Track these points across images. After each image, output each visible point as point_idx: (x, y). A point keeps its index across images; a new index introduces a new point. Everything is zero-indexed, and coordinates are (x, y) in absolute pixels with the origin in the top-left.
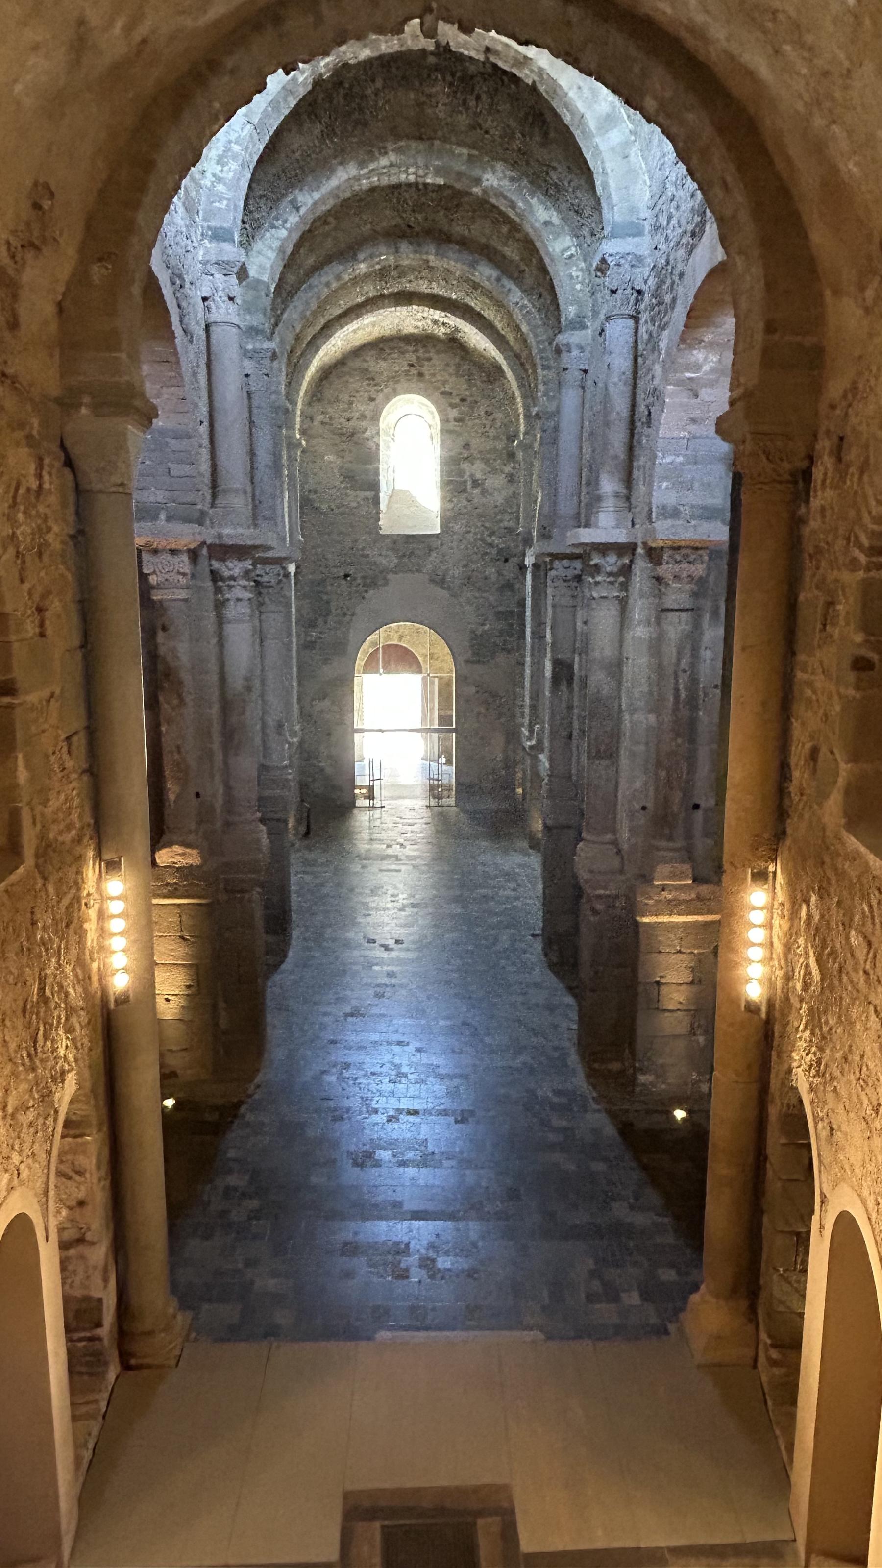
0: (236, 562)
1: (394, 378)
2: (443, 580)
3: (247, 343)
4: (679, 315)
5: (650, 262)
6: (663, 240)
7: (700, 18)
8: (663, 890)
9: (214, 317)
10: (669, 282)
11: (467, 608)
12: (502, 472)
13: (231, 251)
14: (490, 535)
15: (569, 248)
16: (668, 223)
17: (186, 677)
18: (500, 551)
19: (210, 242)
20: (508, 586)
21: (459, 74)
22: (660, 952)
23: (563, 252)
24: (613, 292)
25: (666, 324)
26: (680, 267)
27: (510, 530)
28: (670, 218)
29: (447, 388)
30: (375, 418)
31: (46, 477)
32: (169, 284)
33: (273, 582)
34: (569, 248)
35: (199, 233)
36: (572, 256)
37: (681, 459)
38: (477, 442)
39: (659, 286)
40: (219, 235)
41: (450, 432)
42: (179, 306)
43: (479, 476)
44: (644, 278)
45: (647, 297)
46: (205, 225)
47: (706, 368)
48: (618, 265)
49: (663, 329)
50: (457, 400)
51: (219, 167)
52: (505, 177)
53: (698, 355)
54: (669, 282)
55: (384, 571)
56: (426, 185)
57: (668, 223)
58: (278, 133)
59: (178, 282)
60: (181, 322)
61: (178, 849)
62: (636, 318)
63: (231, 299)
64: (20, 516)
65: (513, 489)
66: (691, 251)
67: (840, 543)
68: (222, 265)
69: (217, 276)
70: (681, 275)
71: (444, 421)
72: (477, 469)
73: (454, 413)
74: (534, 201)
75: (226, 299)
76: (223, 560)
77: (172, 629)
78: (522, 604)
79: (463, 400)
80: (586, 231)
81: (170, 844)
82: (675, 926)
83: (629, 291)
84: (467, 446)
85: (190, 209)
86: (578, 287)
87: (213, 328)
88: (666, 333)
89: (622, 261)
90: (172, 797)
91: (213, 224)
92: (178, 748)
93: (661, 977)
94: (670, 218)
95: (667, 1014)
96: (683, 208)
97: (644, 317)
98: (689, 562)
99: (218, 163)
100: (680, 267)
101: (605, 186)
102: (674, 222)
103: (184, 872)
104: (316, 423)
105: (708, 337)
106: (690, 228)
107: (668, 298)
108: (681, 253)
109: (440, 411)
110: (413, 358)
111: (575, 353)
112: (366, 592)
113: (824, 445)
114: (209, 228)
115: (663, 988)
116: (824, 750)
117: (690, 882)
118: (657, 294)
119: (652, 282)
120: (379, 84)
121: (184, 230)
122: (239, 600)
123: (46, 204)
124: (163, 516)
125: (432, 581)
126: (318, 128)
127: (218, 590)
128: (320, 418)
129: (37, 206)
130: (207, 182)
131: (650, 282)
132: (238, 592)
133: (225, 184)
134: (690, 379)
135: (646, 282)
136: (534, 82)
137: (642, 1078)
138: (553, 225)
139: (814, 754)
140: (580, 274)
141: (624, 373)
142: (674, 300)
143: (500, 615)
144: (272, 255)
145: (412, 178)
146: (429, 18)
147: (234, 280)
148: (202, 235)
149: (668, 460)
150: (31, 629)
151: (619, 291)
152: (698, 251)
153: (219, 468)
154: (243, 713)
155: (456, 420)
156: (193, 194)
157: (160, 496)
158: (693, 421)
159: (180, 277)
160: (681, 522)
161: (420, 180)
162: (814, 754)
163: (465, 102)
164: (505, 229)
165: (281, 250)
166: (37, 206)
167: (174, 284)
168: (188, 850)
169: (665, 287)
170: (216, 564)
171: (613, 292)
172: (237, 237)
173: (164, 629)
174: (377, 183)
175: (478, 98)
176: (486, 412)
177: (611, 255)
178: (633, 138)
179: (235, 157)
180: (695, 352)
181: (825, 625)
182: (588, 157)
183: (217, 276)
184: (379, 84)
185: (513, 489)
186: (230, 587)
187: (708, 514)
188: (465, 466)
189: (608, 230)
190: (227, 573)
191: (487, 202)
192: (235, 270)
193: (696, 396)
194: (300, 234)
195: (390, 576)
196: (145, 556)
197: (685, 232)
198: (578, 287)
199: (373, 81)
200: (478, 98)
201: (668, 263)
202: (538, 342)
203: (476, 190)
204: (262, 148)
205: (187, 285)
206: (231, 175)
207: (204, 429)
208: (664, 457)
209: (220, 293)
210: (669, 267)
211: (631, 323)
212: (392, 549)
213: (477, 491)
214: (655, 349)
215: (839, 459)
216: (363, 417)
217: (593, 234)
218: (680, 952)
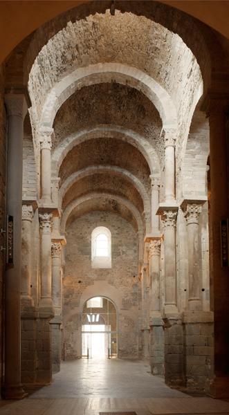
18: (132, 274)
20: (136, 285)
27: (135, 267)
30: (90, 233)
47: (197, 148)
55: (93, 280)
71: (112, 234)
72: (124, 248)
73: (116, 232)
76: (43, 214)
77: (26, 229)
78: (140, 290)
87: (43, 151)
110: (102, 215)
111: (156, 180)
125: (109, 283)
127: (41, 224)
143: (133, 294)
144: (60, 154)
153: (43, 189)
163: (120, 108)
165: (63, 154)
170: (41, 216)
173: (23, 229)
195: (95, 282)
200: (124, 106)
203: (123, 139)
207: (39, 176)
212: (96, 273)
213: (124, 255)
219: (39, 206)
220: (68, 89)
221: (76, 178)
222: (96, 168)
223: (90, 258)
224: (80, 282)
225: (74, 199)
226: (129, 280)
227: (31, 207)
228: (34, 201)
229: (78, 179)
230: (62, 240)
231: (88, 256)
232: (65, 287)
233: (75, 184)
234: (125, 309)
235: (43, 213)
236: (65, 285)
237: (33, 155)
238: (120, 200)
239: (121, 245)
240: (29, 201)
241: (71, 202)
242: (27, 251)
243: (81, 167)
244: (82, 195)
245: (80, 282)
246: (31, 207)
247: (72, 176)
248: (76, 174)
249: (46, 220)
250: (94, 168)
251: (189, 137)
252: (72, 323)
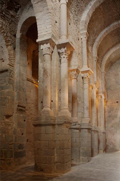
0: (63, 49)
33: (86, 77)
77: (46, 61)
92: (46, 86)
122: (64, 57)
127: (60, 56)
132: (64, 56)
154: (64, 83)
170: (59, 50)
186: (62, 55)
190: (61, 52)
219: (57, 43)
221: (105, 33)
222: (117, 23)
225: (109, 50)
227: (49, 44)
228: (50, 39)
229: (106, 34)
230: (88, 71)
233: (105, 38)
235: (60, 48)
240: (47, 40)
241: (106, 52)
243: (107, 25)
244: (113, 46)
246: (49, 44)
247: (101, 33)
248: (104, 31)
249: (63, 53)
250: (116, 23)
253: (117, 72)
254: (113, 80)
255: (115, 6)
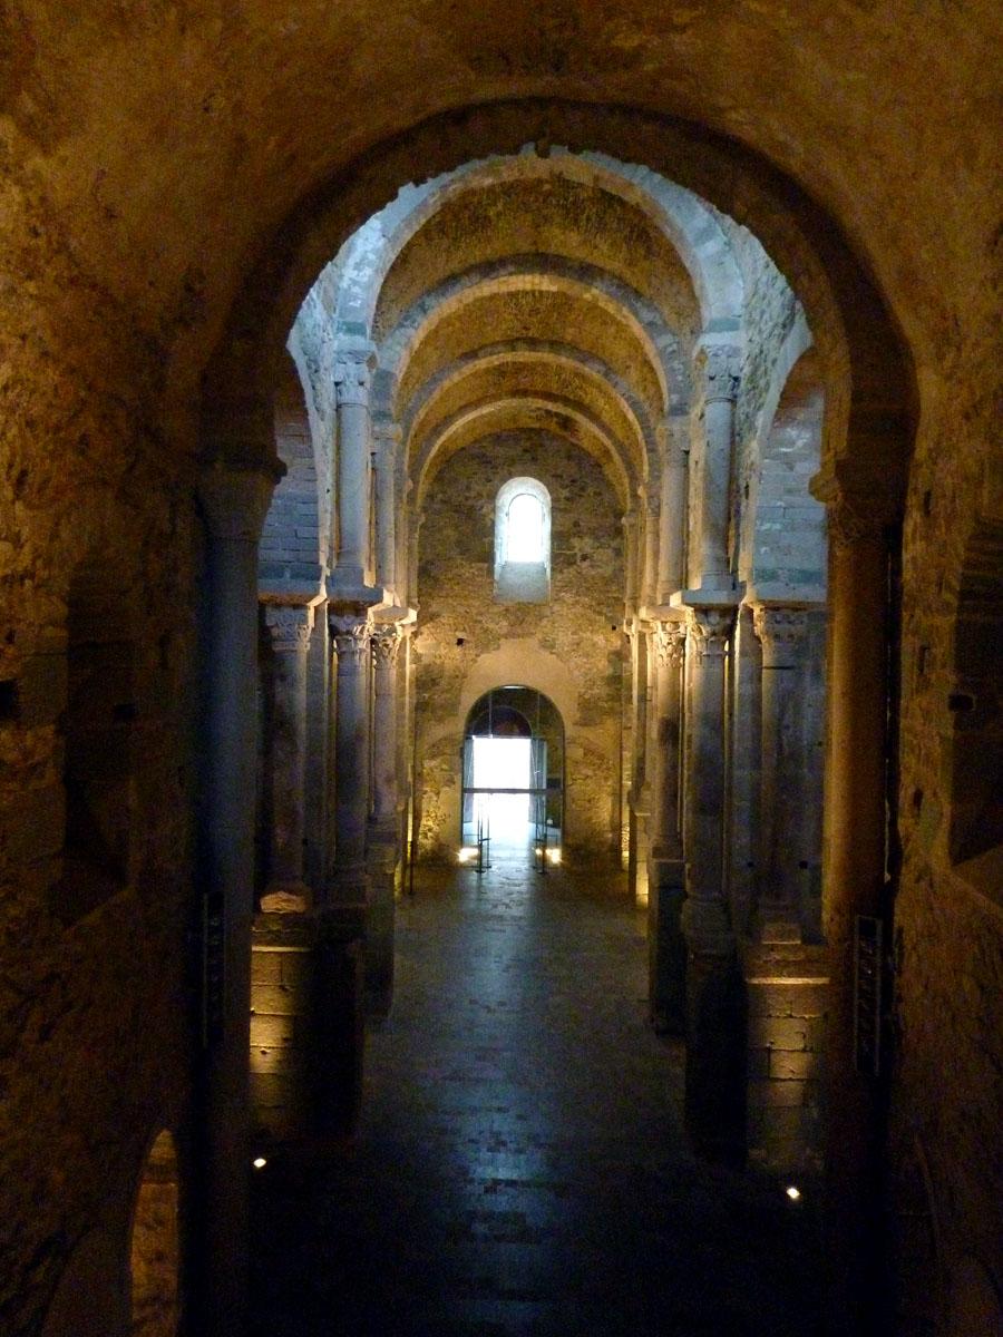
1: (512, 462)
2: (553, 647)
3: (373, 426)
4: (773, 397)
5: (745, 353)
6: (756, 333)
7: (781, 137)
8: (772, 950)
9: (346, 398)
10: (763, 368)
11: (576, 673)
12: (609, 546)
13: (362, 343)
14: (599, 604)
15: (670, 345)
16: (761, 317)
17: (302, 727)
19: (344, 334)
21: (571, 199)
22: (770, 1016)
23: (665, 348)
24: (712, 378)
25: (763, 404)
26: (773, 355)
27: (617, 599)
28: (763, 313)
29: (559, 472)
30: (492, 496)
31: (178, 521)
32: (305, 368)
34: (670, 345)
35: (335, 327)
36: (674, 351)
37: (778, 526)
38: (588, 521)
39: (754, 373)
40: (353, 329)
41: (561, 510)
42: (314, 388)
43: (588, 550)
44: (742, 367)
45: (743, 383)
46: (341, 320)
47: (800, 443)
48: (716, 355)
49: (759, 409)
50: (567, 482)
51: (356, 272)
52: (612, 285)
53: (792, 432)
54: (763, 368)
56: (541, 292)
57: (761, 317)
58: (409, 246)
59: (314, 367)
60: (315, 401)
61: (283, 895)
62: (733, 401)
63: (361, 384)
64: (152, 556)
65: (618, 563)
66: (783, 339)
67: (933, 589)
68: (356, 356)
69: (349, 364)
70: (774, 362)
71: (554, 500)
73: (565, 493)
74: (639, 305)
75: (357, 383)
77: (289, 680)
79: (573, 481)
80: (687, 330)
81: (274, 891)
82: (786, 988)
83: (726, 378)
84: (576, 524)
85: (329, 306)
86: (680, 378)
87: (346, 411)
88: (761, 412)
89: (720, 352)
90: (280, 841)
91: (349, 319)
93: (772, 1043)
94: (763, 313)
95: (778, 1084)
96: (775, 303)
97: (742, 400)
98: (790, 622)
99: (355, 269)
100: (773, 355)
101: (702, 287)
102: (766, 316)
103: (286, 919)
104: (436, 500)
105: (801, 416)
106: (781, 320)
107: (762, 383)
108: (774, 342)
109: (551, 493)
112: (477, 656)
113: (913, 501)
114: (344, 323)
115: (772, 1056)
116: (927, 793)
117: (799, 942)
118: (753, 378)
119: (747, 370)
120: (500, 207)
121: (322, 324)
123: (197, 286)
124: (288, 575)
126: (446, 242)
128: (440, 496)
129: (189, 289)
130: (344, 284)
131: (744, 371)
133: (360, 287)
134: (785, 454)
135: (742, 370)
136: (637, 204)
137: (754, 1153)
138: (656, 324)
139: (918, 798)
140: (681, 366)
141: (722, 450)
142: (768, 384)
145: (528, 287)
146: (542, 143)
147: (364, 367)
148: (338, 329)
149: (767, 526)
150: (153, 657)
151: (717, 378)
152: (789, 340)
155: (567, 499)
156: (332, 293)
157: (287, 556)
158: (790, 492)
159: (315, 362)
160: (779, 584)
161: (537, 288)
162: (918, 798)
164: (613, 330)
166: (189, 289)
167: (309, 367)
168: (294, 897)
169: (759, 373)
170: (335, 619)
171: (712, 378)
172: (369, 331)
174: (496, 291)
175: (588, 219)
176: (595, 493)
177: (708, 347)
178: (727, 248)
179: (370, 264)
180: (789, 429)
181: (922, 670)
182: (687, 265)
183: (349, 364)
184: (500, 207)
185: (618, 563)
187: (807, 577)
188: (575, 542)
189: (705, 325)
191: (596, 307)
192: (366, 359)
193: (791, 469)
194: (426, 333)
195: (503, 640)
196: (269, 610)
197: (776, 325)
198: (680, 378)
199: (495, 205)
201: (761, 352)
202: (642, 428)
204: (394, 257)
205: (322, 371)
206: (366, 279)
208: (761, 525)
209: (352, 379)
210: (763, 356)
211: (727, 405)
213: (587, 563)
214: (752, 427)
215: (927, 513)
216: (480, 495)
217: (692, 332)
218: (791, 1016)
220: (359, 691)
223: (491, 571)
224: (460, 642)
226: (599, 639)
231: (486, 565)
232: (417, 658)
234: (585, 722)
236: (420, 651)
237: (312, 456)
238: (578, 417)
239: (580, 535)
242: (294, 744)
245: (460, 642)
251: (777, 417)
252: (433, 763)
253: (467, 499)
254: (445, 532)
255: (512, 305)
